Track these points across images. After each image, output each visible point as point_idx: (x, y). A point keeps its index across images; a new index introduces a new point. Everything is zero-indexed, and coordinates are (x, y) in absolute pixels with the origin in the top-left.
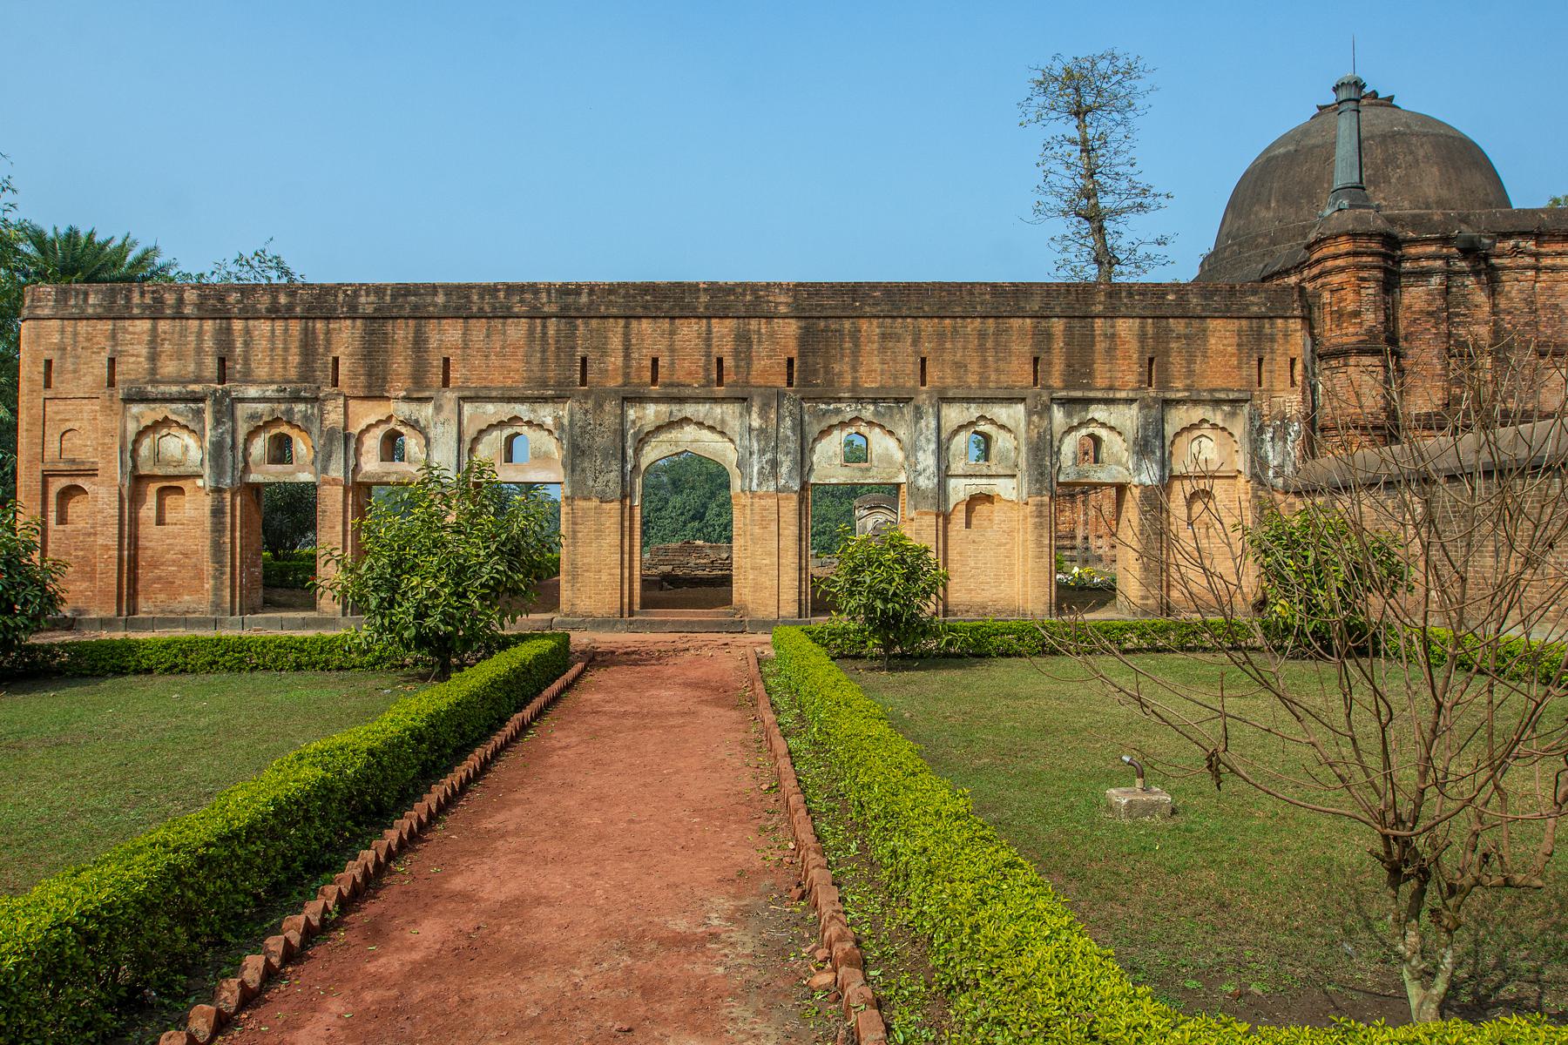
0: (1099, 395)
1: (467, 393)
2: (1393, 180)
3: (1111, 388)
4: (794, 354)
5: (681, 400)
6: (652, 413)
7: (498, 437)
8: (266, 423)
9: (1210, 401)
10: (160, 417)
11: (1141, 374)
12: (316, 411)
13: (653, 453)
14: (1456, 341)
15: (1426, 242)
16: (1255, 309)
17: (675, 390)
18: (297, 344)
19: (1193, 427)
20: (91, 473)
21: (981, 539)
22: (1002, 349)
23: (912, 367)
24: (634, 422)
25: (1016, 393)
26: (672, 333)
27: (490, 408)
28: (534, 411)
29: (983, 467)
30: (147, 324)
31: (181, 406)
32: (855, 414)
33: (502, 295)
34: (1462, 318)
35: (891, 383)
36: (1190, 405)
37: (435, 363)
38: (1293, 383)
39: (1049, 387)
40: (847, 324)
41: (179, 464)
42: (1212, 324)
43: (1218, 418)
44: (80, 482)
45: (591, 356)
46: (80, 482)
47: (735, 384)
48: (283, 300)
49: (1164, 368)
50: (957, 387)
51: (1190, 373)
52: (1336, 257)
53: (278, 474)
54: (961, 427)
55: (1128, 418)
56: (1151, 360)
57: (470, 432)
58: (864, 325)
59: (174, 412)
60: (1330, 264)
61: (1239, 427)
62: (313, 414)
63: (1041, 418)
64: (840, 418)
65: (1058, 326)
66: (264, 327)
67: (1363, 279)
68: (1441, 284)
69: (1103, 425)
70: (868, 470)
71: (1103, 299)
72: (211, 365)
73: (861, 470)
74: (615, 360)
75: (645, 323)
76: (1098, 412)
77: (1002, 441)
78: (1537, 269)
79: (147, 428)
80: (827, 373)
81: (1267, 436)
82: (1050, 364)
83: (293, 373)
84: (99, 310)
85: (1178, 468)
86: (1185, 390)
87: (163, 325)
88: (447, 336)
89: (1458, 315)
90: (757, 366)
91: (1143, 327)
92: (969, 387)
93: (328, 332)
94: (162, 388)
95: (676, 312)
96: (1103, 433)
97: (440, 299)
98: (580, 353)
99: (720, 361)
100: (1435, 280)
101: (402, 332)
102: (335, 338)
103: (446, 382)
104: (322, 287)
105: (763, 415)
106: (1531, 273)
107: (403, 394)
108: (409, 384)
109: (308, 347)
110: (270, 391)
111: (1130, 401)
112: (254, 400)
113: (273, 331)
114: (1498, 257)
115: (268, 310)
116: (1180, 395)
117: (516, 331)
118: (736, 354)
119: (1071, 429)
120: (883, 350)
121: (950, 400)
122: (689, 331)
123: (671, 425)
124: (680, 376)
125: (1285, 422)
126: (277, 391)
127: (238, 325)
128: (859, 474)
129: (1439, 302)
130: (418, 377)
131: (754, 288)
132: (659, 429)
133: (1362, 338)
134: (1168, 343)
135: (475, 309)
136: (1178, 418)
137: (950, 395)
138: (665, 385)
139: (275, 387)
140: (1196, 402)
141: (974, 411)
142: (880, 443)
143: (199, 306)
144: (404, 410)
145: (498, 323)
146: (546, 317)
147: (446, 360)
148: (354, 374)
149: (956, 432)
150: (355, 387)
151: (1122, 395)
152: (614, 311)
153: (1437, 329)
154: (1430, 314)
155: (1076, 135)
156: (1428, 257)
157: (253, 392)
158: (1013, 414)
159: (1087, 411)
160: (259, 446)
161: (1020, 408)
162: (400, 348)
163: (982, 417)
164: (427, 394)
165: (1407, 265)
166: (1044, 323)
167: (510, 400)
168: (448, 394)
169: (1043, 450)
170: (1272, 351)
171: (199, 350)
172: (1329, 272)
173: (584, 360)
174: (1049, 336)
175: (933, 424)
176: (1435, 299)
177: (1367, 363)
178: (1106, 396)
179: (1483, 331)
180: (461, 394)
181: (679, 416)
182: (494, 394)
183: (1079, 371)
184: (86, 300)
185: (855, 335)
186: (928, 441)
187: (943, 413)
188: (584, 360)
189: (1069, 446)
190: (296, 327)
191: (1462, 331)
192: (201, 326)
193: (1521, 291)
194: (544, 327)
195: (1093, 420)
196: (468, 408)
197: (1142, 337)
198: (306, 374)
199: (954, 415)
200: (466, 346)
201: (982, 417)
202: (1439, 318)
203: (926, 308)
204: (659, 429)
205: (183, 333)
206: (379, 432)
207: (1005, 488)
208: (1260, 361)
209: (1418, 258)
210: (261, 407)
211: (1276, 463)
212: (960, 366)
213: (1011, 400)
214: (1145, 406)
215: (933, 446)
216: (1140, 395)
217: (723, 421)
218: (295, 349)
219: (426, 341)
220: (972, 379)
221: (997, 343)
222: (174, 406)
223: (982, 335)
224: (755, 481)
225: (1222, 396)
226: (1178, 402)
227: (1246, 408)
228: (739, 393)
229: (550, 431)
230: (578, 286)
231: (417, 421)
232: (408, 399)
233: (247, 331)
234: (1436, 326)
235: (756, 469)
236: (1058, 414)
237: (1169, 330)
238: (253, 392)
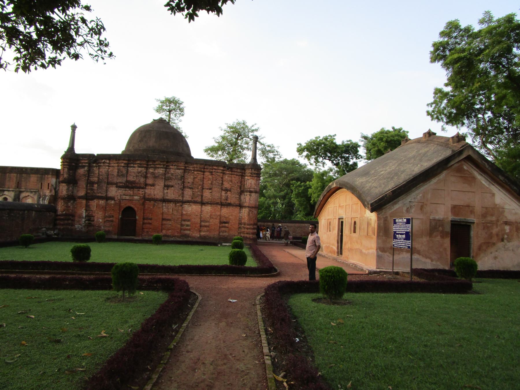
2: (144, 141)
3: (9, 188)
19: (26, 197)
34: (92, 176)
38: (48, 188)
42: (31, 175)
43: (32, 195)
56: (18, 182)
67: (64, 168)
69: (7, 195)
76: (6, 193)
78: (109, 166)
81: (41, 199)
89: (91, 175)
91: (17, 176)
96: (8, 197)
100: (86, 168)
106: (107, 167)
111: (13, 191)
125: (45, 196)
129: (87, 173)
140: (27, 192)
151: (11, 189)
154: (84, 175)
156: (85, 163)
165: (80, 165)
179: (96, 179)
193: (105, 171)
197: (17, 178)
209: (83, 163)
214: (15, 192)
216: (15, 190)
225: (32, 190)
226: (23, 191)
227: (37, 194)
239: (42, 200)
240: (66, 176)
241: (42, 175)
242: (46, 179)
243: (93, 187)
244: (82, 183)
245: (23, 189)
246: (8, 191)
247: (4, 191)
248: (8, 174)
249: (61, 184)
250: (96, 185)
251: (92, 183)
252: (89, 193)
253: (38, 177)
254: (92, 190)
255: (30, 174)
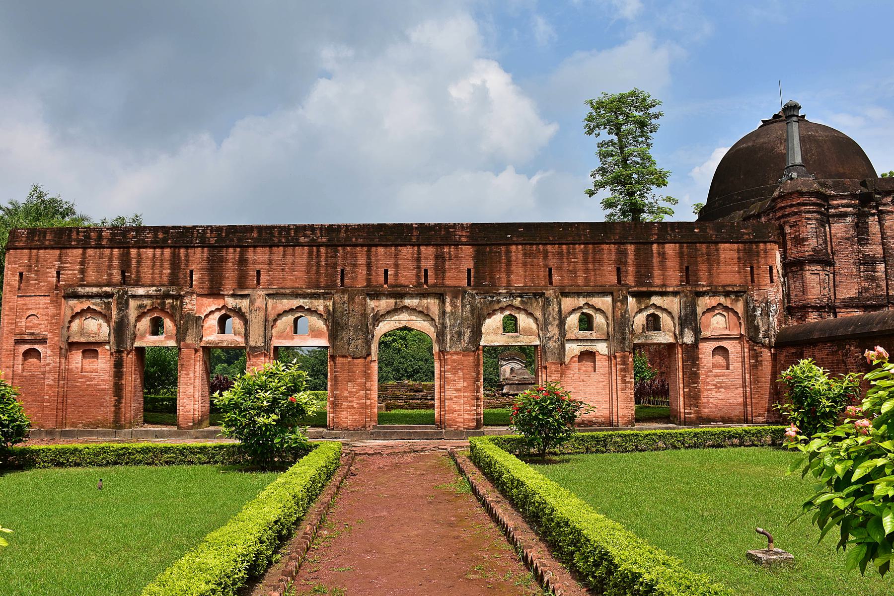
0: (657, 289)
1: (271, 292)
3: (664, 285)
4: (471, 267)
5: (401, 296)
6: (384, 304)
7: (290, 318)
8: (148, 310)
9: (723, 292)
10: (85, 307)
11: (681, 276)
12: (178, 303)
13: (383, 327)
14: (863, 254)
15: (843, 197)
16: (746, 237)
17: (399, 289)
18: (168, 262)
19: (714, 308)
20: (43, 341)
21: (586, 379)
22: (598, 263)
23: (543, 274)
24: (373, 309)
25: (607, 289)
26: (396, 255)
27: (285, 301)
28: (311, 303)
29: (587, 334)
30: (80, 251)
31: (98, 301)
32: (510, 303)
33: (292, 232)
35: (530, 283)
36: (711, 294)
37: (252, 273)
39: (627, 285)
40: (503, 249)
41: (96, 335)
44: (36, 347)
45: (347, 269)
46: (36, 347)
47: (435, 285)
48: (161, 235)
49: (696, 274)
50: (571, 286)
51: (711, 276)
52: (792, 206)
53: (154, 342)
54: (574, 310)
55: (674, 304)
56: (687, 268)
57: (272, 316)
58: (513, 248)
59: (93, 304)
60: (788, 211)
61: (739, 307)
62: (177, 305)
63: (622, 304)
64: (500, 305)
65: (631, 249)
66: (150, 252)
67: (809, 219)
68: (852, 221)
69: (660, 308)
70: (517, 337)
71: (656, 232)
72: (117, 277)
73: (513, 337)
74: (362, 272)
75: (381, 250)
76: (656, 300)
77: (599, 319)
79: (77, 313)
80: (491, 278)
81: (758, 313)
82: (627, 270)
83: (165, 280)
84: (52, 243)
85: (705, 334)
86: (708, 286)
87: (90, 252)
88: (258, 256)
89: (863, 239)
90: (448, 275)
91: (681, 248)
92: (579, 286)
93: (187, 255)
94: (88, 289)
95: (399, 241)
97: (255, 234)
98: (339, 267)
99: (426, 271)
100: (849, 219)
101: (231, 256)
102: (191, 259)
103: (259, 283)
104: (184, 227)
105: (454, 305)
107: (231, 292)
108: (235, 285)
109: (175, 264)
110: (152, 290)
111: (675, 294)
112: (141, 296)
113: (154, 254)
114: (884, 205)
115: (152, 242)
116: (705, 289)
117: (302, 253)
118: (436, 266)
119: (640, 311)
120: (525, 263)
121: (565, 294)
122: (407, 253)
123: (397, 310)
124: (402, 281)
126: (156, 291)
127: (133, 252)
128: (512, 340)
129: (852, 232)
130: (242, 283)
131: (447, 227)
132: (388, 313)
133: (810, 253)
134: (696, 258)
135: (276, 240)
136: (705, 302)
137: (567, 290)
138: (391, 286)
139: (154, 288)
140: (714, 293)
141: (582, 301)
142: (524, 321)
143: (110, 240)
144: (231, 302)
145: (289, 251)
146: (319, 246)
147: (258, 272)
148: (201, 279)
149: (571, 313)
150: (203, 288)
151: (670, 289)
152: (360, 241)
153: (852, 248)
155: (615, 138)
156: (844, 206)
157: (141, 291)
158: (605, 302)
159: (650, 299)
160: (145, 323)
161: (609, 299)
162: (230, 265)
163: (587, 304)
164: (246, 292)
165: (832, 211)
166: (622, 247)
167: (297, 296)
168: (260, 292)
169: (622, 323)
170: (758, 262)
171: (110, 267)
172: (788, 215)
173: (343, 271)
174: (626, 254)
175: (556, 309)
176: (849, 230)
177: (814, 268)
178: (661, 290)
180: (267, 292)
181: (402, 305)
182: (288, 291)
183: (644, 273)
184: (45, 237)
185: (508, 253)
186: (554, 319)
187: (563, 303)
188: (343, 271)
189: (640, 320)
190: (167, 251)
191: (866, 248)
192: (111, 253)
194: (318, 251)
195: (654, 304)
196: (270, 302)
197: (681, 254)
198: (174, 280)
199: (568, 303)
200: (270, 263)
201: (587, 304)
202: (853, 241)
203: (551, 238)
204: (389, 313)
205: (101, 256)
206: (217, 315)
207: (602, 348)
208: (752, 268)
210: (147, 302)
211: (763, 329)
212: (574, 272)
213: (604, 293)
215: (557, 322)
217: (428, 308)
218: (167, 265)
219: (246, 260)
220: (580, 280)
221: (594, 258)
222: (93, 301)
223: (585, 253)
224: (448, 345)
228: (437, 290)
229: (321, 315)
230: (339, 226)
231: (240, 309)
232: (234, 296)
233: (139, 255)
234: (851, 245)
235: (449, 337)
236: (631, 300)
237: (696, 250)
238: (141, 291)
239: (761, 314)
240: (813, 242)
241: (751, 242)
242: (762, 253)
243: (875, 272)
244: (845, 262)
245: (704, 286)
246: (663, 294)
247: (650, 294)
248: (655, 246)
249: (808, 268)
250: (881, 267)
251: (869, 261)
252: (866, 290)
253: (738, 251)
254: (873, 279)
255: (717, 243)
